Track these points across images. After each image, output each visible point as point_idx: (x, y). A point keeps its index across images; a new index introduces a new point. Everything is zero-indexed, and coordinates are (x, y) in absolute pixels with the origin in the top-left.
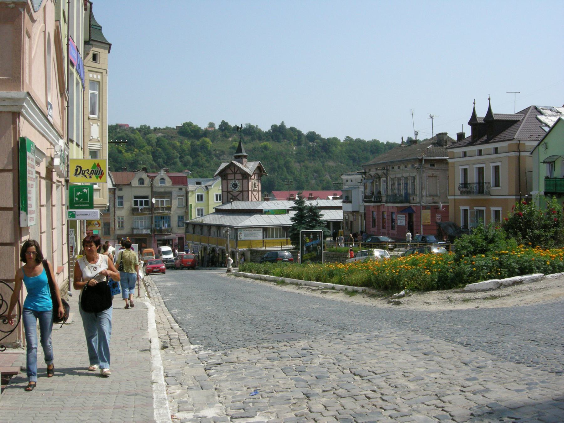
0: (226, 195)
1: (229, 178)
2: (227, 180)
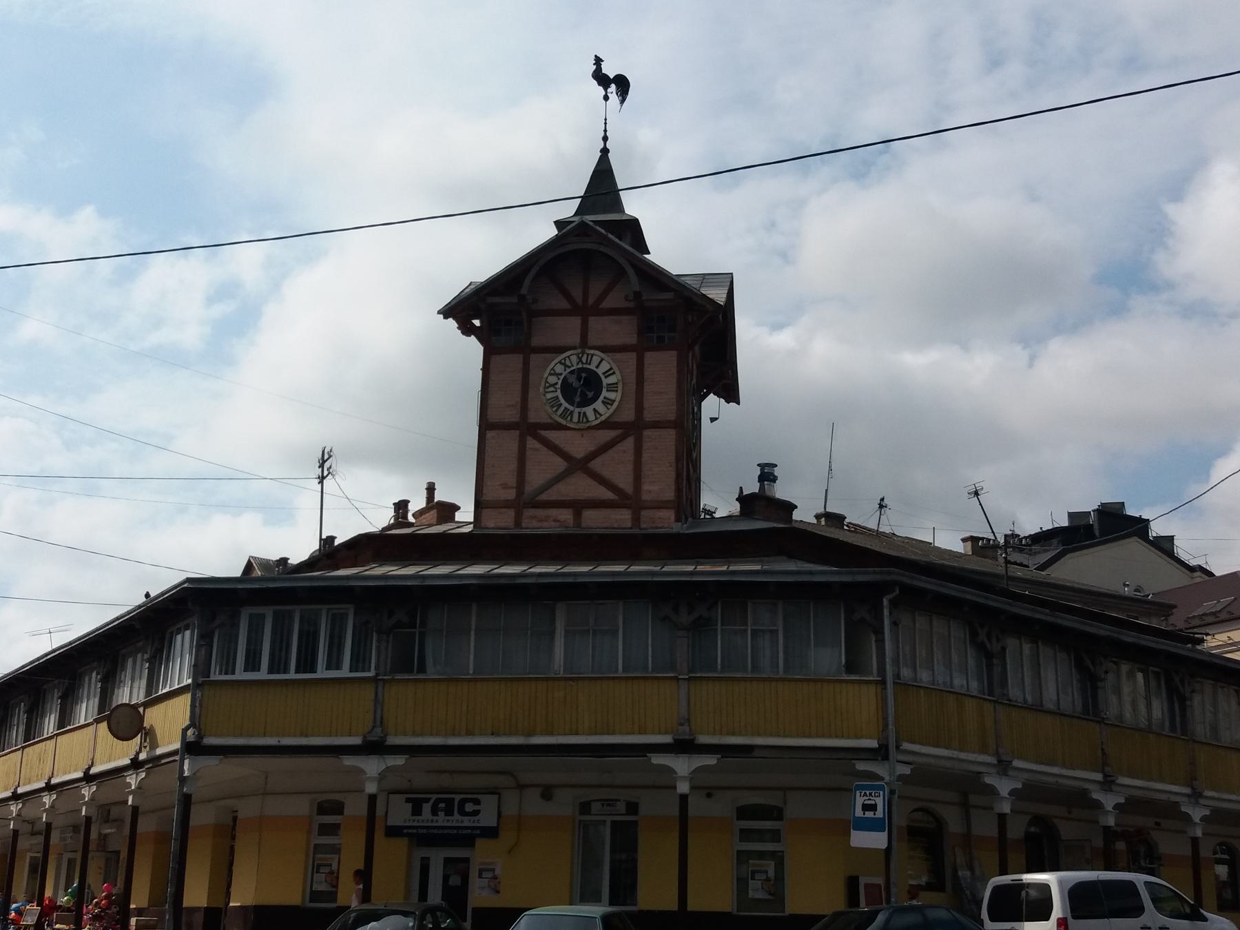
1: (535, 342)
2: (526, 349)
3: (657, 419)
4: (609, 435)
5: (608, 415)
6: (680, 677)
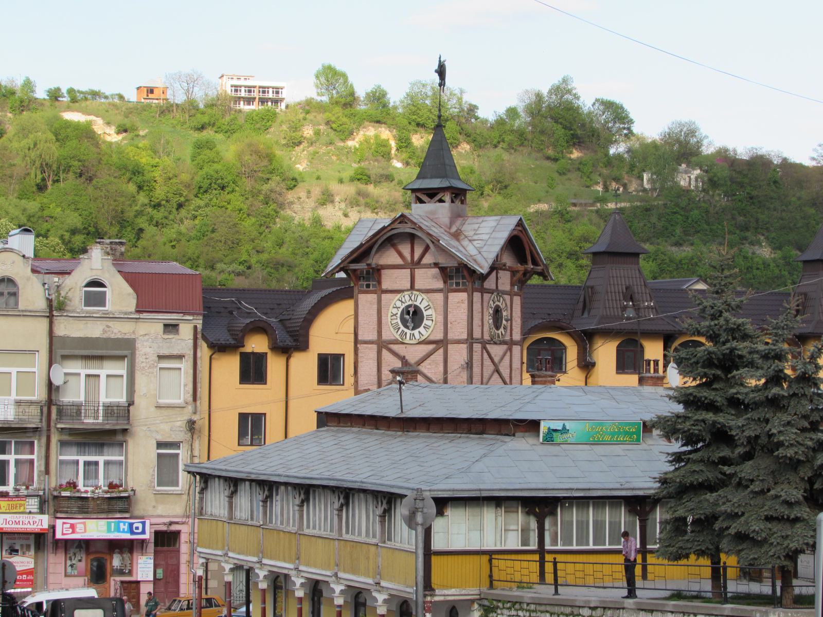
0: (374, 355)
1: (385, 285)
4: (431, 347)
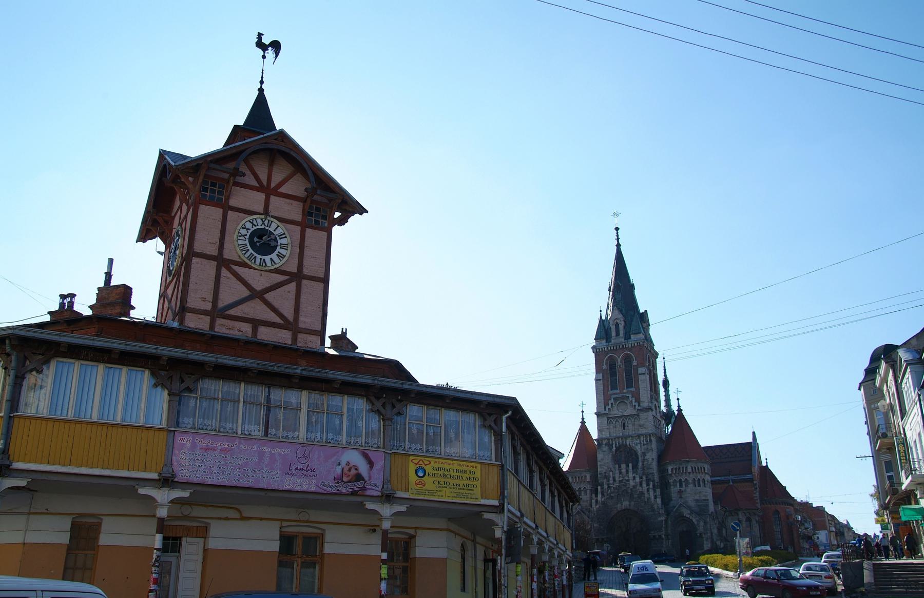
0: (213, 273)
1: (233, 202)
2: (227, 208)
3: (313, 275)
4: (281, 278)
5: (280, 264)
6: (386, 452)
